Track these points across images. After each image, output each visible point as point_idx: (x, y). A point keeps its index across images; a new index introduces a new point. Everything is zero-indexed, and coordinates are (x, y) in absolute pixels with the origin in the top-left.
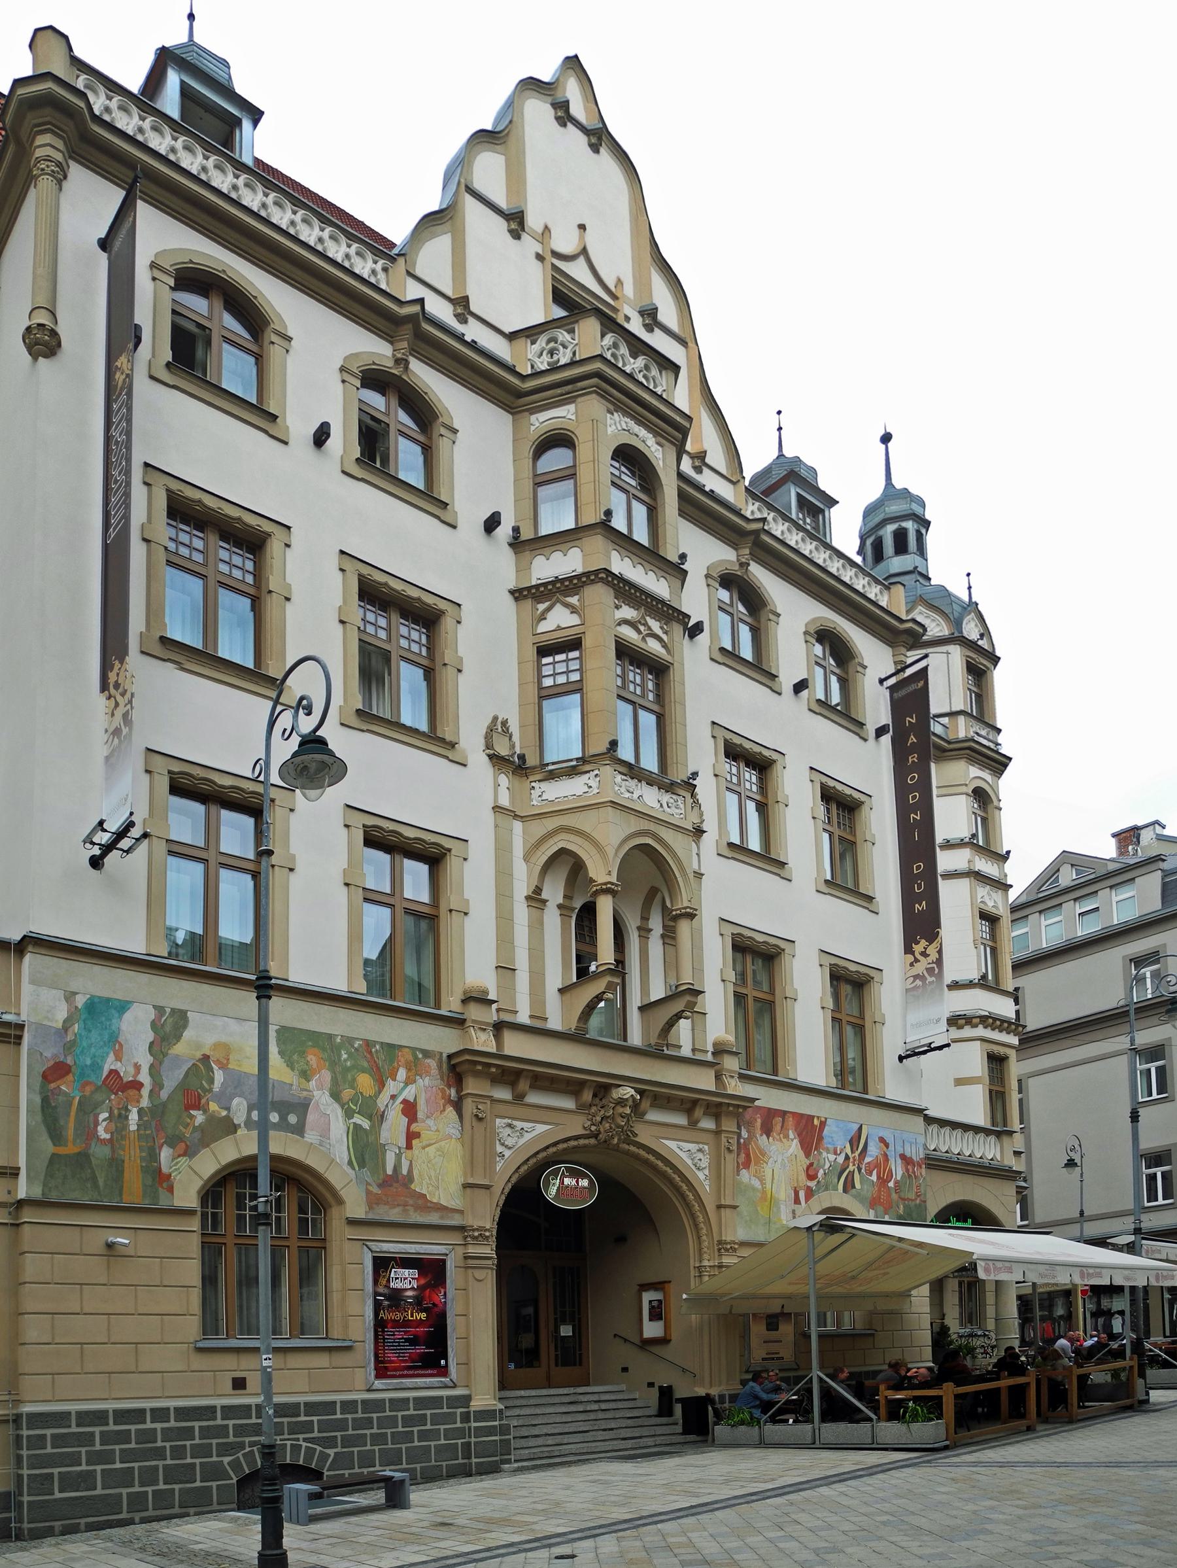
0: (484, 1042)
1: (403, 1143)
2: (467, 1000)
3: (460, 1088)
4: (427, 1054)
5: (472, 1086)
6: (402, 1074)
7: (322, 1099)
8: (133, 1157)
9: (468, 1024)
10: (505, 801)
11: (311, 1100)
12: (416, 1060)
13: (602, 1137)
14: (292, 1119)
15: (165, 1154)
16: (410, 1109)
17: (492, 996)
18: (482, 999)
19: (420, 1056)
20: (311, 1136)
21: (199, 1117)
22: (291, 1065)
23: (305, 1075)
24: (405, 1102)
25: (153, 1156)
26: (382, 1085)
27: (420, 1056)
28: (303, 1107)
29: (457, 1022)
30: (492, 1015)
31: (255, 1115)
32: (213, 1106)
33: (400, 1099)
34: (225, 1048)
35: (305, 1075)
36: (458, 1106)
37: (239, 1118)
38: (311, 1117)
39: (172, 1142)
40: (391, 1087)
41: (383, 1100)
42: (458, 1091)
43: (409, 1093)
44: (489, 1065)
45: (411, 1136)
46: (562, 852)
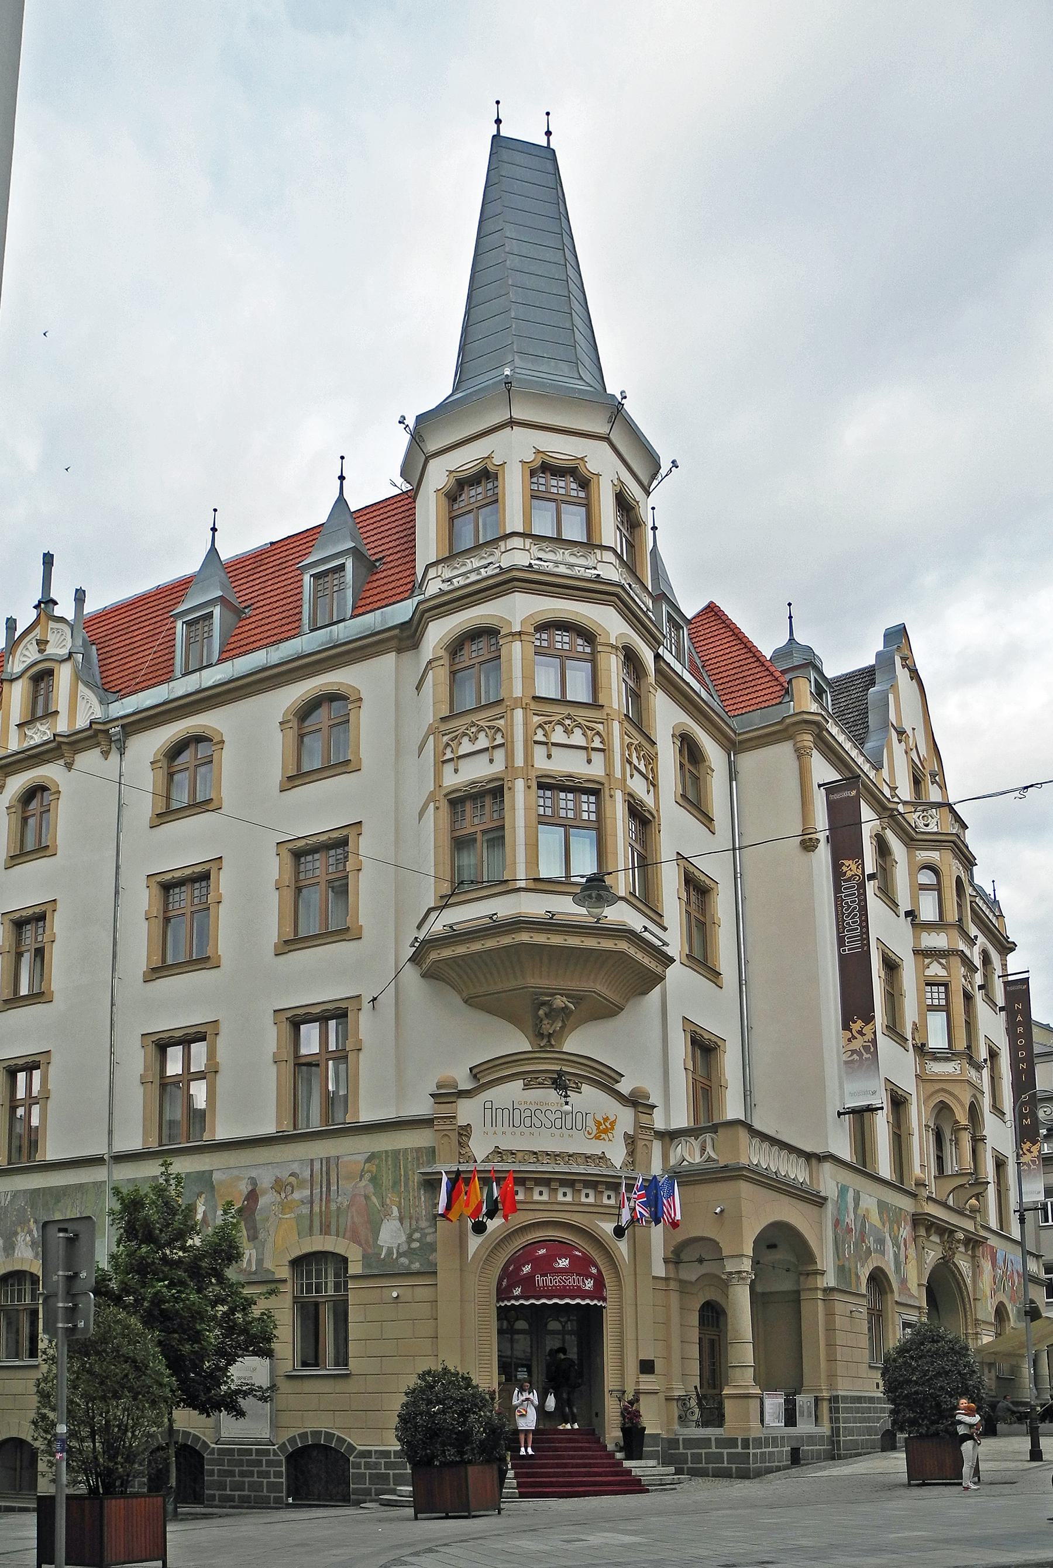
8: (853, 1265)
13: (947, 1259)
35: (884, 1225)
44: (929, 1220)
45: (906, 1258)
46: (941, 1101)
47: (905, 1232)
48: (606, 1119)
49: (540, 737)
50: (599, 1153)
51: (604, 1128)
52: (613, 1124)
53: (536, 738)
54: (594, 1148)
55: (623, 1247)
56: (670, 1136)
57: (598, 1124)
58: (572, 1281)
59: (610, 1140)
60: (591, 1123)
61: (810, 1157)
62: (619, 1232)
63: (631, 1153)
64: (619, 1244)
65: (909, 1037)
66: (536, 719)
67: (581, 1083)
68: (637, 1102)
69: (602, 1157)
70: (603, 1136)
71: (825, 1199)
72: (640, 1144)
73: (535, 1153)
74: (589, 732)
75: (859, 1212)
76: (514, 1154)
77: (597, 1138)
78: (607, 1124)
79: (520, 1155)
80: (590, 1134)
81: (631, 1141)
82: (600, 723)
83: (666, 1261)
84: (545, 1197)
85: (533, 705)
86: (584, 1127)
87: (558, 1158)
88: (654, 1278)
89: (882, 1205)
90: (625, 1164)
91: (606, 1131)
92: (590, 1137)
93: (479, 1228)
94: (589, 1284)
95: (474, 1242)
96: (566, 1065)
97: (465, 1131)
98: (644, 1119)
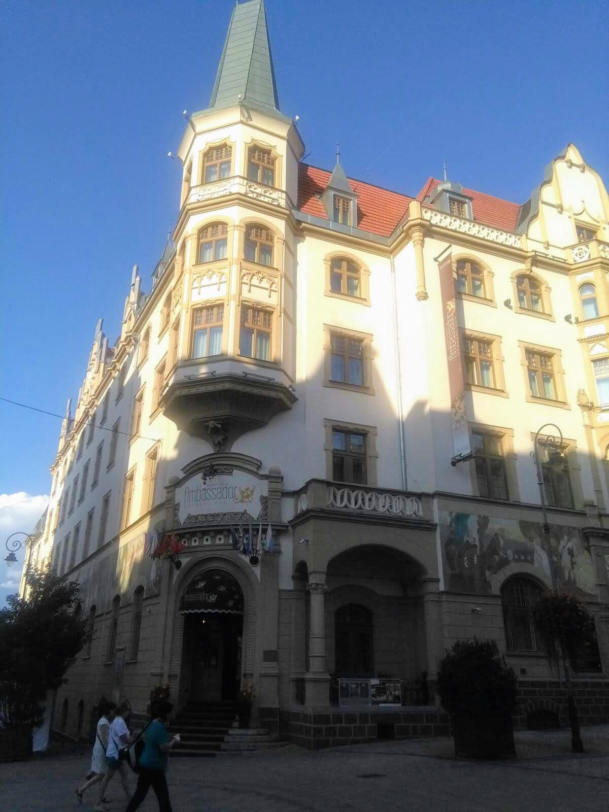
0: (593, 523)
1: (570, 566)
2: (586, 506)
3: (588, 543)
4: (574, 529)
5: (592, 542)
6: (566, 537)
7: (538, 548)
9: (588, 515)
10: (587, 422)
11: (534, 550)
12: (570, 531)
14: (529, 558)
15: (487, 573)
16: (571, 553)
17: (595, 504)
18: (592, 506)
19: (571, 530)
20: (536, 565)
21: (497, 558)
22: (525, 535)
23: (531, 540)
24: (569, 549)
25: (483, 574)
26: (559, 542)
27: (571, 530)
28: (532, 553)
29: (583, 514)
30: (596, 512)
31: (516, 557)
32: (501, 554)
33: (566, 549)
34: (502, 530)
35: (531, 540)
36: (588, 549)
37: (511, 558)
38: (536, 556)
39: (489, 569)
40: (563, 543)
41: (561, 547)
42: (588, 543)
43: (570, 545)
47: (568, 543)
48: (247, 490)
49: (196, 285)
50: (243, 511)
51: (246, 495)
52: (252, 491)
53: (194, 286)
54: (239, 508)
55: (257, 570)
56: (296, 494)
57: (243, 492)
58: (202, 596)
59: (250, 502)
60: (237, 492)
61: (420, 496)
62: (254, 561)
63: (265, 507)
64: (254, 569)
65: (572, 400)
66: (195, 276)
67: (233, 470)
68: (275, 477)
69: (245, 513)
70: (246, 500)
71: (436, 525)
72: (270, 502)
73: (206, 516)
74: (220, 274)
75: (487, 532)
76: (195, 517)
77: (242, 501)
78: (248, 492)
79: (200, 518)
80: (237, 500)
81: (264, 501)
82: (225, 268)
83: (294, 578)
84: (209, 543)
85: (193, 269)
86: (234, 497)
87: (217, 517)
88: (280, 591)
89: (525, 526)
90: (261, 516)
91: (248, 497)
92: (237, 501)
93: (178, 565)
94: (213, 598)
95: (176, 573)
96: (214, 461)
97: (176, 508)
98: (274, 485)
